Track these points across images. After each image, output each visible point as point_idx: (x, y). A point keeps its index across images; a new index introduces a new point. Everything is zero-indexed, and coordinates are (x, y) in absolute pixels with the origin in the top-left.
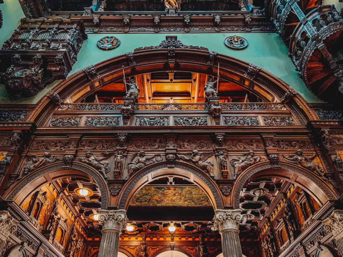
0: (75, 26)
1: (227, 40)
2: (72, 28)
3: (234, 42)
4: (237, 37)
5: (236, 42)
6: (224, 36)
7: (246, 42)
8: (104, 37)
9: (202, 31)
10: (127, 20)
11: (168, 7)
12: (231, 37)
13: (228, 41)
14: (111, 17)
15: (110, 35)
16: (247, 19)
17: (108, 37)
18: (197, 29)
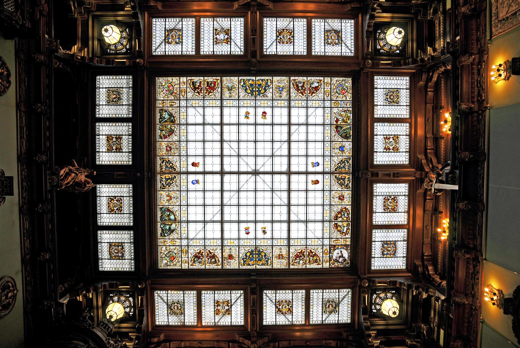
0: (28, 25)
1: (10, 279)
2: (24, 19)
3: (6, 292)
4: (14, 296)
5: (6, 295)
6: (17, 273)
7: (7, 312)
8: (10, 68)
9: (24, 234)
10: (40, 108)
11: (62, 172)
12: (15, 286)
13: (8, 282)
14: (44, 81)
15: (13, 79)
16: (46, 303)
17: (9, 75)
18: (27, 225)
